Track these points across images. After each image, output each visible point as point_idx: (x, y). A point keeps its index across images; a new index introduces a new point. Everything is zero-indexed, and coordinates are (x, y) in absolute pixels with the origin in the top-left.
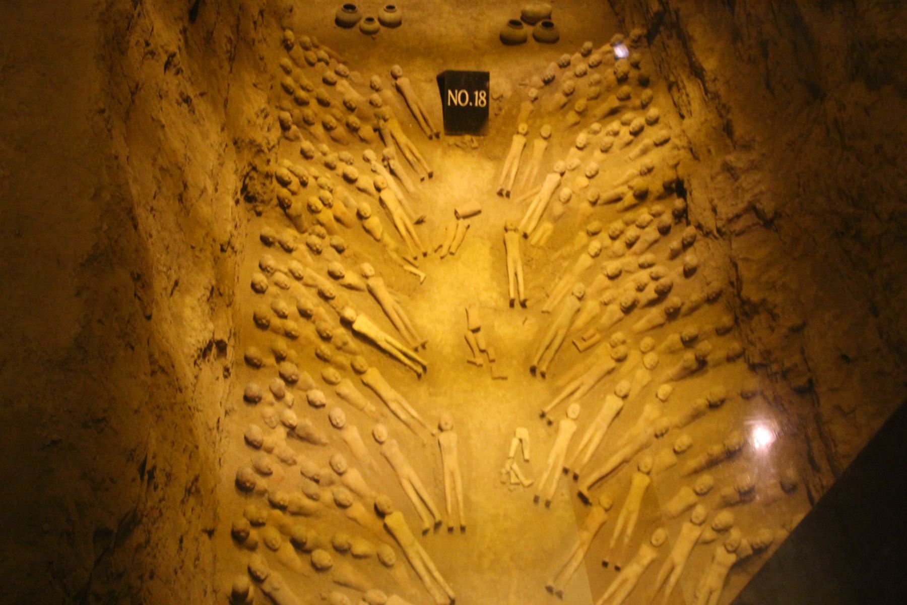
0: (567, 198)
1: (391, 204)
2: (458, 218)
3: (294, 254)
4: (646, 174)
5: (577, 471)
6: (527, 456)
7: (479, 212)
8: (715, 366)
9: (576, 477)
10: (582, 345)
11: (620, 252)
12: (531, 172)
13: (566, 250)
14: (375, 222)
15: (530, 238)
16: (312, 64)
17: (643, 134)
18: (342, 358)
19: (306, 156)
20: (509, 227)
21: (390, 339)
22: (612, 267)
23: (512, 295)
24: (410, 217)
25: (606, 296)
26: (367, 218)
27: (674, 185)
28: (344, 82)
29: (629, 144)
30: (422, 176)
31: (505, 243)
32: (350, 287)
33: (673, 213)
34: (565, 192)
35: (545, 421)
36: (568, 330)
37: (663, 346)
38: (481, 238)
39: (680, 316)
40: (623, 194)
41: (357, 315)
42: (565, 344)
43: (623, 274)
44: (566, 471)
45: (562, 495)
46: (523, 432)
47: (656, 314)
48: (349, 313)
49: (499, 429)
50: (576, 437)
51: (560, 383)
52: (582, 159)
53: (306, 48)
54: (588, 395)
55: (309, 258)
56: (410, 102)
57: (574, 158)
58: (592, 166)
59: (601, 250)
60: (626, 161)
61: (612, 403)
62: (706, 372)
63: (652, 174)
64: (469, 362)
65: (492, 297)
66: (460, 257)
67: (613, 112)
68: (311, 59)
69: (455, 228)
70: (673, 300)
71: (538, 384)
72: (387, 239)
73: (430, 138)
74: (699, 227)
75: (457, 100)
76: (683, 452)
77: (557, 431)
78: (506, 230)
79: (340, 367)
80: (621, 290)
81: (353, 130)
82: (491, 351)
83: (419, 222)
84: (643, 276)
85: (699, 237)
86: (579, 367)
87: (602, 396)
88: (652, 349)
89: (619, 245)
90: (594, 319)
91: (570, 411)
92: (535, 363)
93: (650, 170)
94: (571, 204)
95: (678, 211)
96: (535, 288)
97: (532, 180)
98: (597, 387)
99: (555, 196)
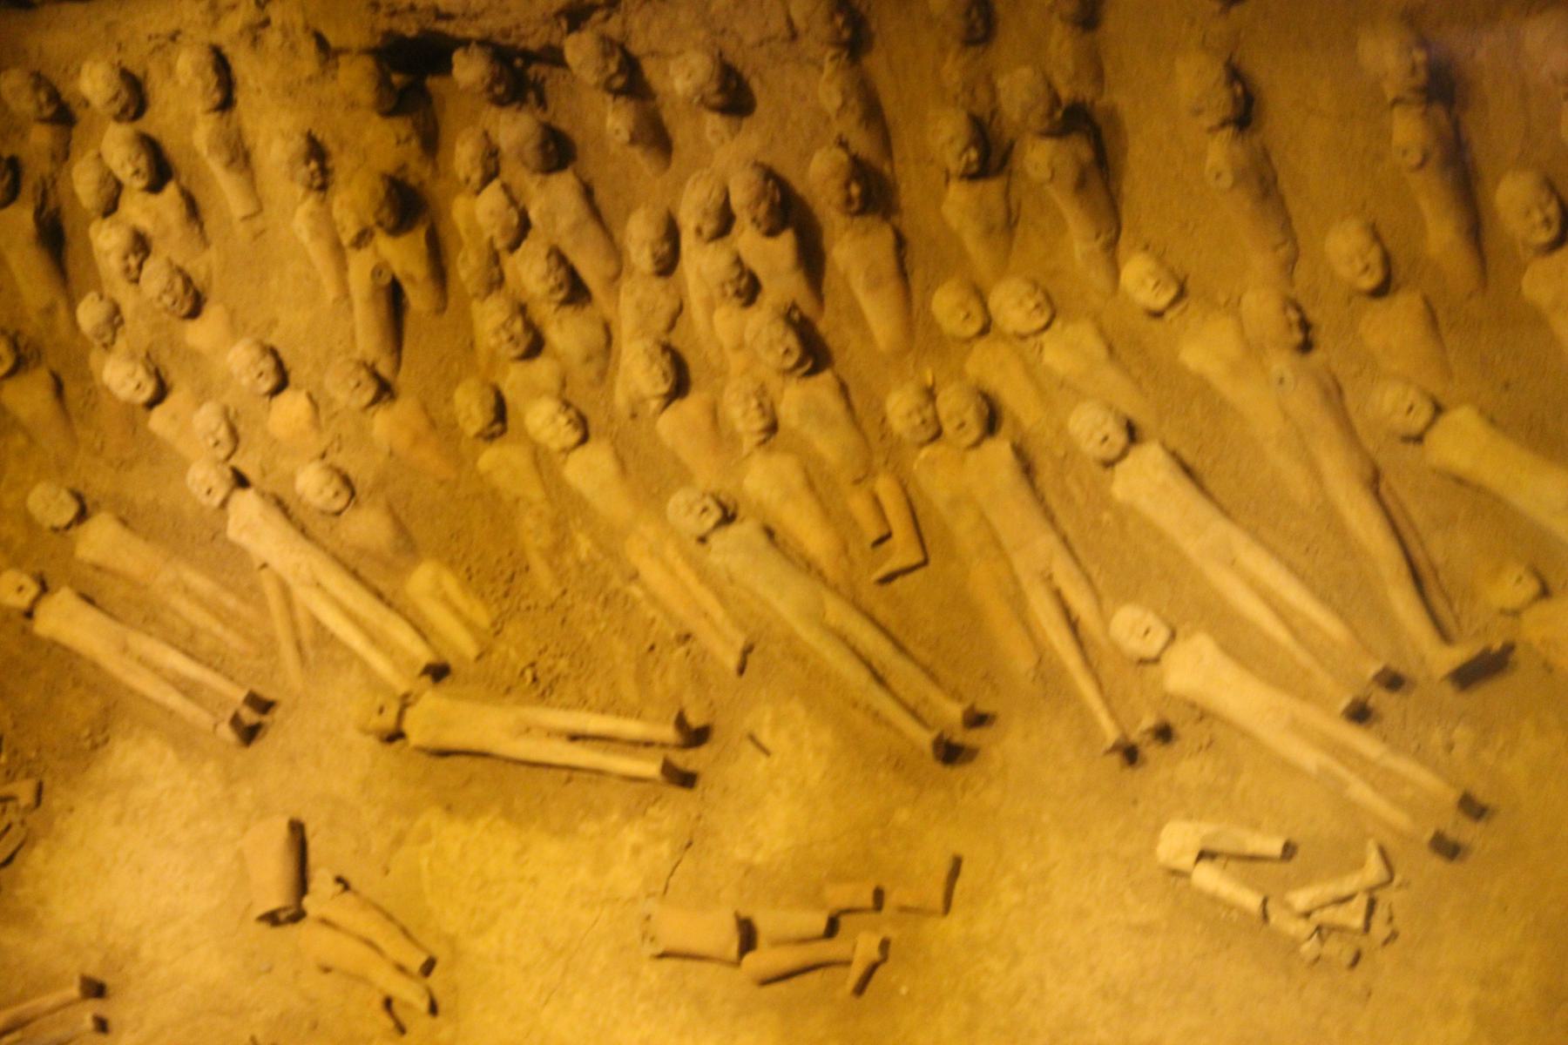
0: (336, 483)
2: (298, 916)
4: (324, 171)
5: (1373, 669)
6: (1274, 846)
7: (297, 830)
8: (1099, 77)
9: (1393, 681)
10: (902, 552)
11: (595, 335)
12: (200, 601)
13: (533, 535)
15: (451, 660)
17: (171, 145)
20: (389, 720)
22: (639, 373)
23: (649, 767)
25: (743, 419)
27: (396, 79)
29: (193, 209)
30: (88, 1023)
31: (444, 753)
33: (499, 102)
34: (311, 484)
35: (1152, 751)
36: (835, 589)
37: (979, 254)
38: (399, 841)
39: (886, 169)
40: (377, 272)
42: (881, 612)
43: (676, 340)
44: (1360, 714)
45: (1450, 747)
46: (1177, 841)
47: (853, 252)
49: (1147, 930)
50: (1240, 646)
51: (1022, 662)
52: (202, 395)
54: (1094, 570)
57: (189, 426)
58: (241, 363)
59: (567, 405)
60: (258, 235)
61: (1145, 481)
62: (1112, 114)
63: (332, 146)
64: (860, 989)
65: (637, 850)
66: (452, 941)
67: (54, 237)
69: (336, 933)
70: (820, 177)
71: (1009, 746)
76: (1387, 260)
77: (1203, 714)
78: (395, 736)
80: (736, 362)
82: (840, 896)
84: (703, 265)
85: (613, 27)
86: (982, 581)
87: (1106, 516)
88: (980, 294)
89: (567, 334)
90: (815, 482)
91: (1137, 646)
92: (925, 739)
93: (316, 151)
95: (496, 80)
96: (641, 678)
97: (230, 601)
98: (1069, 528)
99: (319, 527)
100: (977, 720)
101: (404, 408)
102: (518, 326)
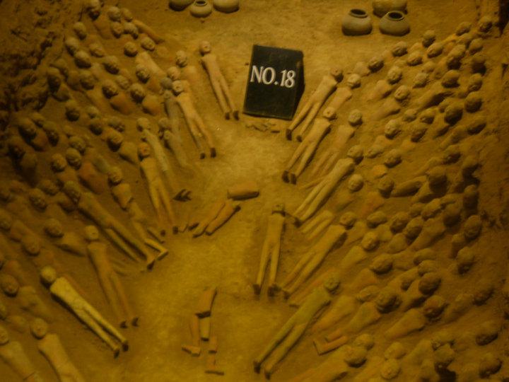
1: (150, 174)
3: (10, 205)
10: (322, 347)
14: (124, 189)
15: (303, 226)
16: (117, 36)
18: (18, 319)
19: (71, 117)
21: (89, 308)
22: (380, 259)
23: (259, 282)
24: (169, 190)
26: (117, 184)
28: (145, 54)
29: (442, 133)
32: (69, 250)
41: (58, 276)
48: (48, 272)
53: (113, 19)
55: (28, 213)
56: (213, 79)
68: (116, 30)
70: (436, 300)
72: (135, 208)
73: (227, 118)
74: (485, 217)
75: (261, 78)
79: (15, 329)
81: (138, 99)
83: (182, 198)
85: (485, 229)
89: (398, 239)
90: (346, 317)
93: (454, 158)
94: (360, 193)
99: (343, 184)
100: (268, 376)
101: (381, 200)
102: (399, 224)
